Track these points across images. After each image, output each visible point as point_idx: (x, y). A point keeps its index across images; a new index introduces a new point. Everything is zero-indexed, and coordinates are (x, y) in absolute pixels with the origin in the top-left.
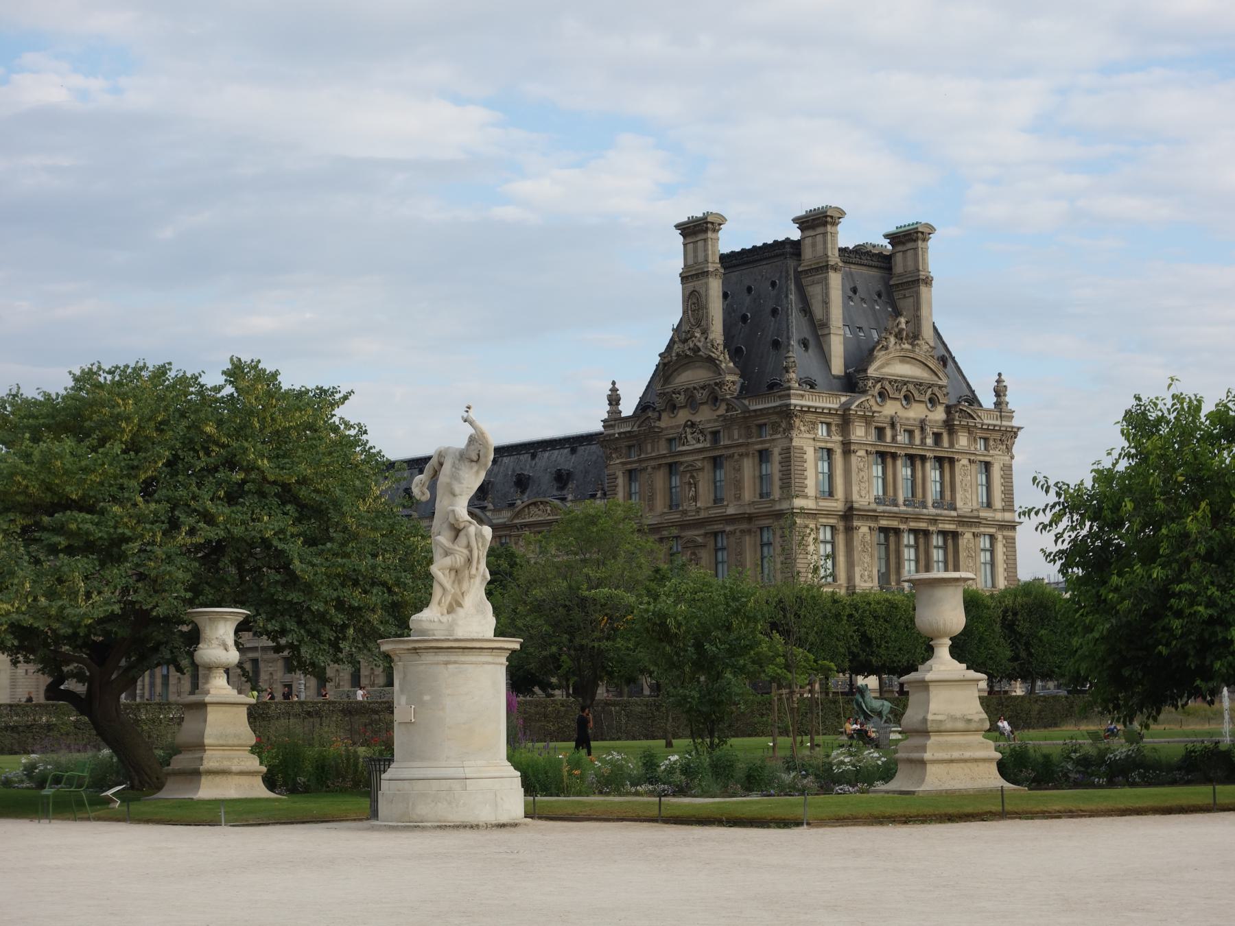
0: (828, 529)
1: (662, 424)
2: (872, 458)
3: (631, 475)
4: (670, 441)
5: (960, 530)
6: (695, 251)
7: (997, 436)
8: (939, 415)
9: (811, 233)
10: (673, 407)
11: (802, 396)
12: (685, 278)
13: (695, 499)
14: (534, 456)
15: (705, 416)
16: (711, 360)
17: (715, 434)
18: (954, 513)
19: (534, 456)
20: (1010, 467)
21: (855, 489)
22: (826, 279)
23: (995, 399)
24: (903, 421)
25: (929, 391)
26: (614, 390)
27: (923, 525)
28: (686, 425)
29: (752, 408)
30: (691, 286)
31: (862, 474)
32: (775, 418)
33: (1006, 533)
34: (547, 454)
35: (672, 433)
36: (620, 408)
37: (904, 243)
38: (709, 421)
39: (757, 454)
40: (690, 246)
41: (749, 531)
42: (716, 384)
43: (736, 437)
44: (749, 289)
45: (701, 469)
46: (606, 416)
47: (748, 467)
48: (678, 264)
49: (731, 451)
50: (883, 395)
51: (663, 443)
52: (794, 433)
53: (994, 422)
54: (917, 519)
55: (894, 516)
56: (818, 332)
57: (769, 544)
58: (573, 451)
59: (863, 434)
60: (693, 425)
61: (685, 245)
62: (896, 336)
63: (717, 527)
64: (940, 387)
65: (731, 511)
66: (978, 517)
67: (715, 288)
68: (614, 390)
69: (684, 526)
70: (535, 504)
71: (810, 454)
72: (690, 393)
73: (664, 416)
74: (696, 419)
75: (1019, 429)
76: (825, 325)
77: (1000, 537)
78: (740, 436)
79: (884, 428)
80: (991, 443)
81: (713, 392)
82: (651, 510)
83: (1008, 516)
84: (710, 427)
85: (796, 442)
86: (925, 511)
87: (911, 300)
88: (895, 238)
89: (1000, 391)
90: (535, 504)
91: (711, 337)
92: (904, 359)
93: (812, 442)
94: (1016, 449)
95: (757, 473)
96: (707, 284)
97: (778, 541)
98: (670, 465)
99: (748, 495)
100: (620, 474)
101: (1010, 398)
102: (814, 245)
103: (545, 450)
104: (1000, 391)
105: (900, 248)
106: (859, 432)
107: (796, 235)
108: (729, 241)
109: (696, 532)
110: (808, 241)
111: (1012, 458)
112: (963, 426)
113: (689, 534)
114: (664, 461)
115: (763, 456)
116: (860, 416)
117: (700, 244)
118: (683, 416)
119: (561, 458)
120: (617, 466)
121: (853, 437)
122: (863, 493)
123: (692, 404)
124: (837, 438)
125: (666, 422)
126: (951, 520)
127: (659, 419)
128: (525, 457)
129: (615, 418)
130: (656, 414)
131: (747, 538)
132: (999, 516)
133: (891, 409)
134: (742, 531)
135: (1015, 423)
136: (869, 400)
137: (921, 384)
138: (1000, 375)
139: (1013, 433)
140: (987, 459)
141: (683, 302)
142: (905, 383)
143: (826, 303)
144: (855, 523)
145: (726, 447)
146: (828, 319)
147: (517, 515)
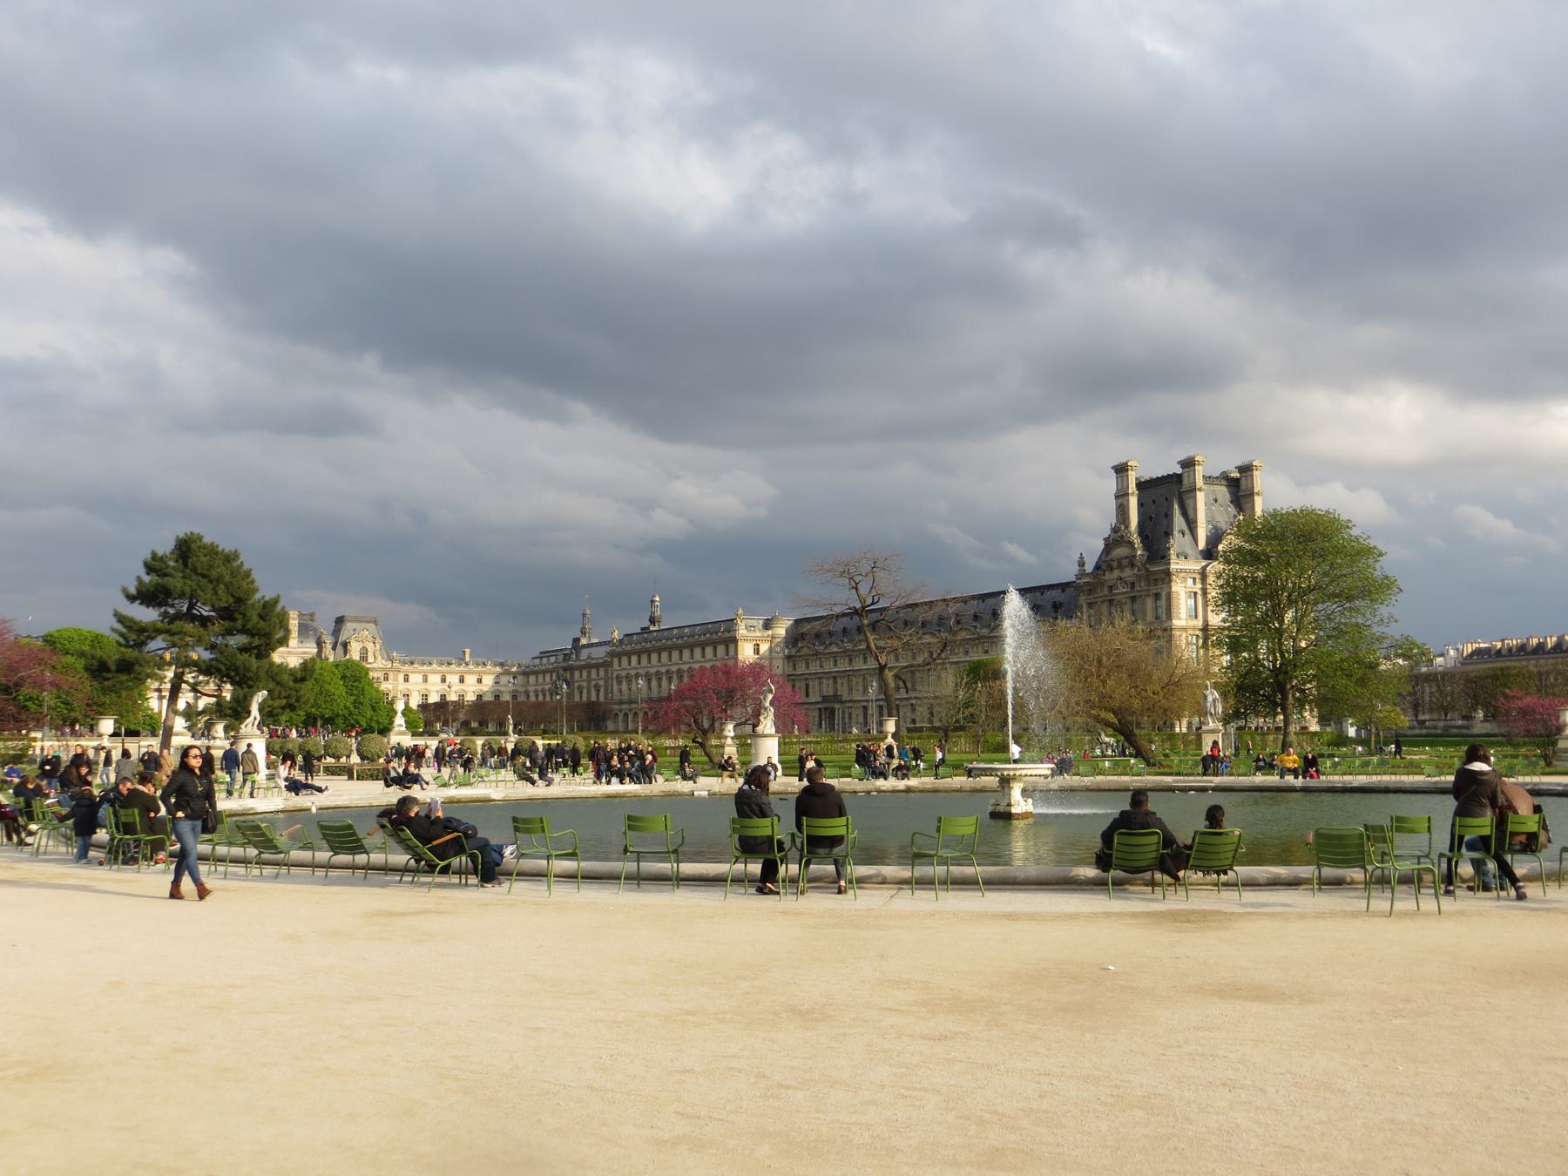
4: (1111, 588)
10: (1111, 569)
15: (1128, 573)
17: (1133, 584)
47: (1149, 602)
107: (1179, 471)
118: (1116, 573)
125: (1108, 576)
129: (1082, 574)
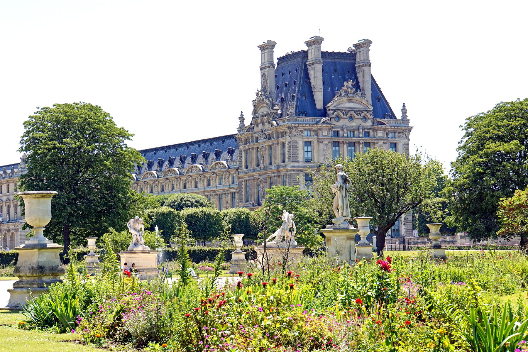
2: (330, 145)
12: (261, 69)
20: (408, 144)
30: (263, 71)
34: (228, 141)
40: (263, 55)
42: (269, 114)
44: (290, 72)
45: (265, 150)
50: (338, 117)
60: (262, 132)
68: (242, 114)
70: (217, 163)
75: (412, 127)
87: (361, 73)
89: (404, 110)
92: (349, 102)
99: (279, 160)
101: (409, 115)
104: (404, 110)
105: (358, 50)
107: (305, 48)
108: (279, 52)
110: (310, 51)
111: (409, 140)
118: (261, 126)
127: (254, 128)
135: (410, 125)
139: (410, 129)
140: (395, 141)
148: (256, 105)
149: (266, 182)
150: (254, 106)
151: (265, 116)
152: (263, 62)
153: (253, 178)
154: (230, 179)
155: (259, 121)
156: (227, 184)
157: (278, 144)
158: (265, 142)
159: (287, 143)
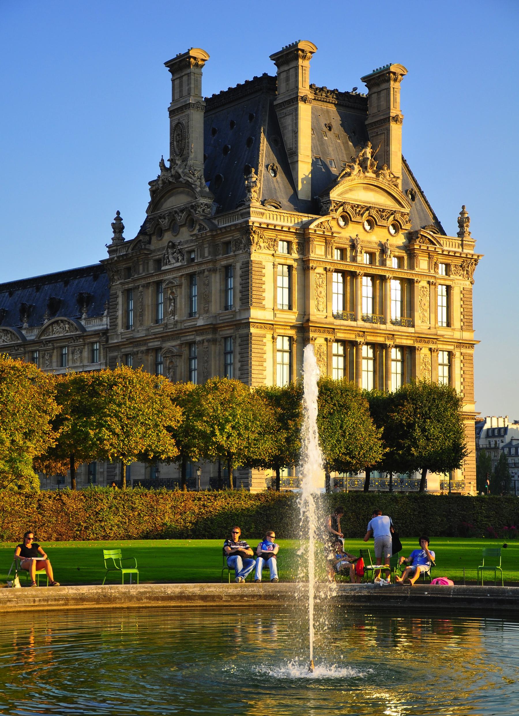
0: (286, 339)
1: (152, 247)
3: (128, 293)
5: (417, 345)
6: (181, 85)
7: (459, 262)
8: (400, 240)
9: (286, 68)
10: (160, 233)
11: (263, 214)
12: (172, 112)
13: (173, 313)
14: (66, 283)
16: (188, 185)
18: (411, 330)
19: (66, 283)
21: (313, 303)
22: (296, 110)
23: (458, 230)
24: (363, 244)
25: (392, 218)
26: (119, 219)
27: (380, 340)
28: (168, 247)
29: (221, 226)
31: (320, 289)
32: (237, 235)
33: (464, 350)
34: (76, 281)
35: (158, 255)
36: (124, 235)
37: (378, 85)
38: (187, 242)
39: (223, 270)
40: (177, 82)
41: (214, 341)
42: (192, 207)
43: (206, 255)
44: (232, 124)
45: (180, 286)
46: (110, 242)
47: (216, 282)
48: (166, 99)
49: (204, 267)
51: (151, 263)
52: (253, 248)
53: (456, 250)
54: (375, 333)
55: (351, 330)
56: (287, 160)
57: (231, 352)
58: (96, 278)
59: (323, 253)
60: (173, 246)
61: (173, 81)
62: (360, 164)
63: (190, 338)
64: (403, 214)
65: (200, 322)
66: (436, 335)
67: (196, 121)
68: (119, 219)
69: (164, 338)
70: (57, 322)
71: (268, 271)
72: (172, 215)
73: (154, 239)
74: (177, 240)
76: (295, 153)
77: (457, 354)
78: (209, 253)
79: (346, 249)
80: (453, 268)
81: (189, 214)
82: (141, 325)
83: (467, 336)
84: (186, 247)
85: (254, 257)
86: (383, 327)
87: (383, 137)
88: (369, 80)
90: (57, 322)
91: (190, 162)
93: (271, 258)
94: (475, 276)
95: (223, 287)
96: (188, 115)
97: (238, 349)
98: (158, 284)
99: (215, 307)
100: (120, 294)
102: (287, 79)
103: (75, 278)
105: (375, 90)
106: (317, 250)
107: (272, 71)
109: (174, 343)
112: (423, 251)
113: (168, 344)
114: (152, 280)
115: (228, 271)
116: (319, 236)
117: (185, 79)
118: (168, 237)
119: (85, 285)
120: (118, 286)
121: (312, 256)
122: (321, 307)
123: (174, 228)
124: (295, 255)
126: (409, 336)
127: (149, 242)
128: (61, 284)
129: (118, 244)
130: (147, 238)
131: (213, 347)
132: (457, 335)
133: (352, 231)
134: (208, 341)
136: (330, 222)
137: (384, 211)
138: (463, 207)
140: (448, 283)
141: (171, 134)
142: (368, 209)
143: (295, 132)
144: (312, 335)
145: (200, 264)
146: (297, 148)
147: (43, 332)
148: (160, 191)
149: (180, 356)
150: (153, 193)
151: (182, 211)
152: (177, 97)
153: (144, 348)
154: (86, 354)
155: (165, 223)
156: (78, 364)
157: (214, 270)
158: (179, 269)
159: (238, 265)
